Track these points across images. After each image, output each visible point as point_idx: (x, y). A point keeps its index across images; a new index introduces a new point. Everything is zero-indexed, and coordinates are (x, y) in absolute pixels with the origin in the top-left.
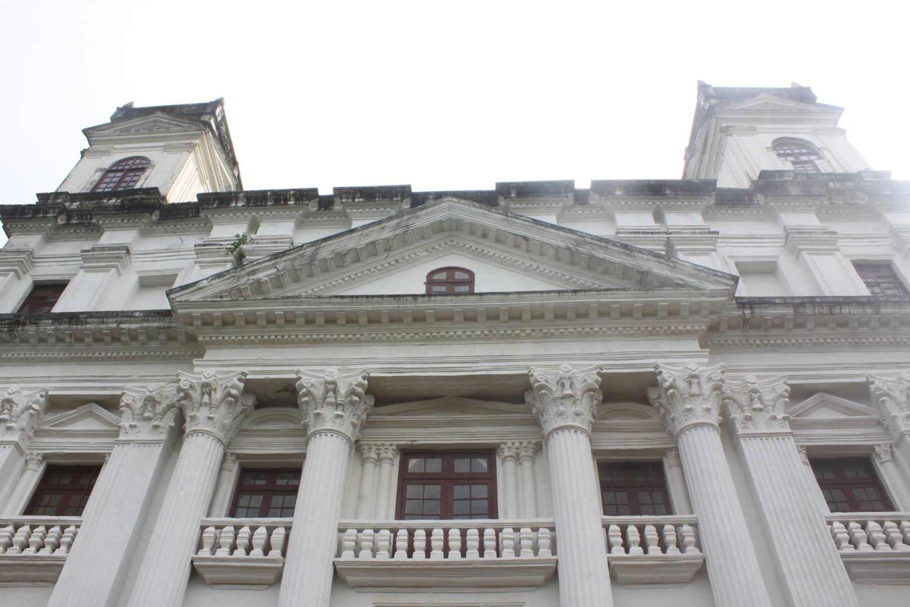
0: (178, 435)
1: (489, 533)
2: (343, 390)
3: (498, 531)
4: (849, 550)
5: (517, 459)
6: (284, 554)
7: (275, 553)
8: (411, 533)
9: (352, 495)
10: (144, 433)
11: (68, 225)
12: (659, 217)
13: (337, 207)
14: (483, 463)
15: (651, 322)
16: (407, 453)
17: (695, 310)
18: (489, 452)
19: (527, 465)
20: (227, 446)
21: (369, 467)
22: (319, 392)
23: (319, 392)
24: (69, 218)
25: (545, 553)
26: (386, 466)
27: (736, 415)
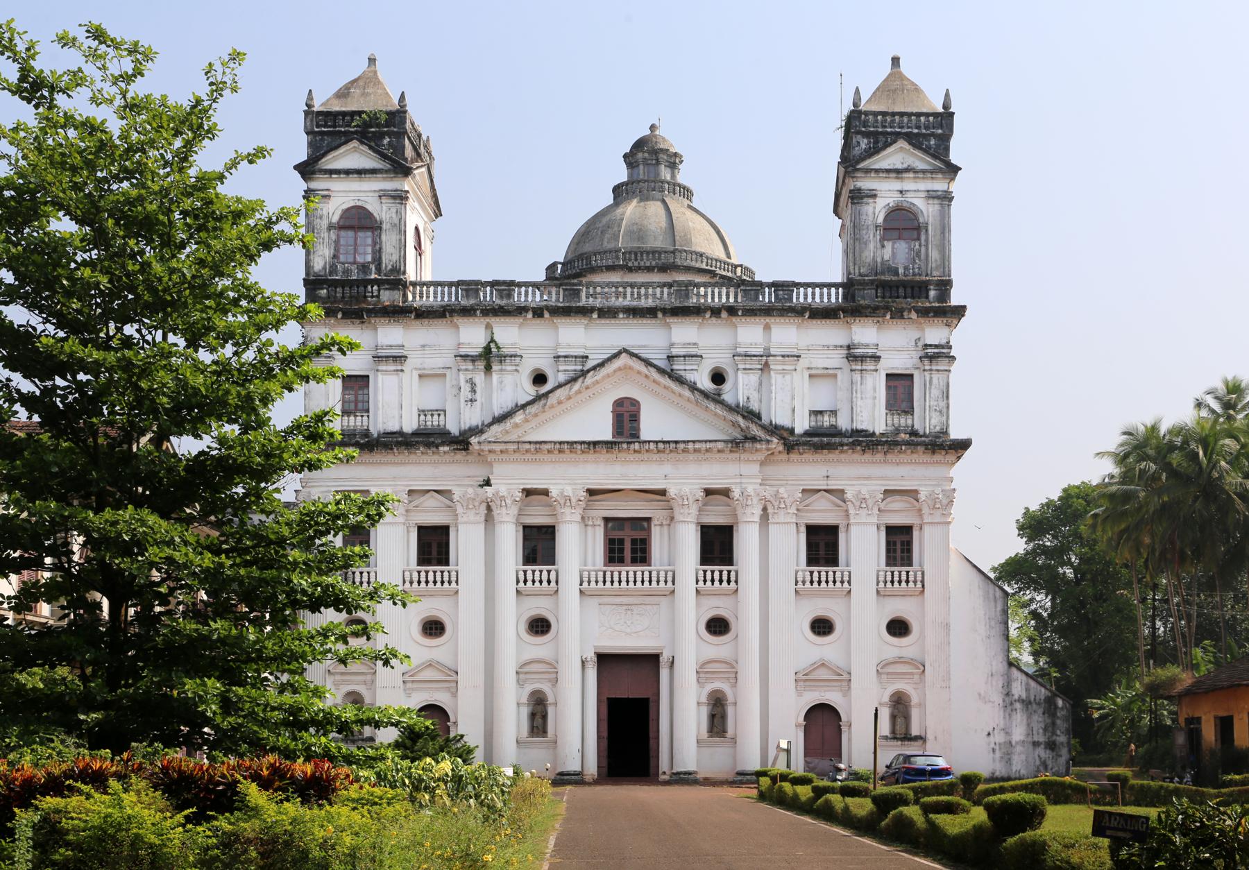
0: (489, 518)
1: (646, 575)
2: (574, 500)
3: (650, 573)
5: (661, 525)
6: (557, 582)
7: (553, 584)
8: (612, 573)
10: (471, 516)
12: (767, 328)
13: (547, 315)
14: (645, 524)
18: (648, 520)
19: (666, 528)
20: (518, 523)
21: (589, 528)
22: (562, 502)
23: (562, 502)
25: (670, 583)
27: (770, 510)
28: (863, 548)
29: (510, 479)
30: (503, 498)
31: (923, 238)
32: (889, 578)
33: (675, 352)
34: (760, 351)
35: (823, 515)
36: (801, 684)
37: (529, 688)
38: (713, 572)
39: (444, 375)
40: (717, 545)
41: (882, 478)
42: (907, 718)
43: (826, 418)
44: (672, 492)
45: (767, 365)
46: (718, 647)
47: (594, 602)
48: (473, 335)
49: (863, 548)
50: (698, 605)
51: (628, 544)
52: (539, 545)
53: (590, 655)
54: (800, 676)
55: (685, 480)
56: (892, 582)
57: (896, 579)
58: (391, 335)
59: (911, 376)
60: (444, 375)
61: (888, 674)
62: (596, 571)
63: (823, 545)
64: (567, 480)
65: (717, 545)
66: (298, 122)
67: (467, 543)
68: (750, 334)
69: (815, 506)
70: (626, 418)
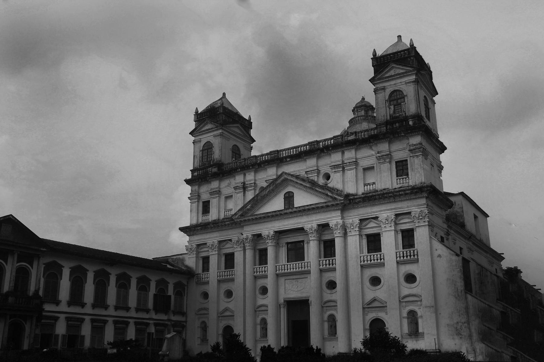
4: (362, 263)
9: (277, 258)
11: (202, 181)
15: (329, 209)
16: (288, 243)
17: (337, 204)
18: (303, 241)
24: (202, 180)
26: (284, 248)
28: (390, 242)
29: (249, 231)
30: (246, 239)
31: (406, 100)
32: (402, 255)
33: (308, 170)
34: (341, 163)
35: (371, 229)
36: (367, 309)
37: (260, 317)
38: (329, 260)
39: (232, 196)
40: (328, 248)
41: (395, 209)
42: (417, 324)
43: (371, 186)
44: (307, 227)
45: (343, 168)
46: (328, 295)
47: (282, 280)
48: (239, 179)
49: (390, 242)
50: (321, 276)
51: (296, 252)
52: (262, 257)
53: (282, 301)
54: (366, 306)
55: (310, 222)
56: (403, 257)
57: (412, 254)
58: (215, 184)
59: (407, 160)
60: (232, 196)
61: (406, 302)
62: (284, 265)
63: (374, 242)
64: (268, 229)
65: (328, 248)
66: (192, 117)
67: (238, 258)
68: (336, 158)
69: (368, 226)
70: (289, 198)
